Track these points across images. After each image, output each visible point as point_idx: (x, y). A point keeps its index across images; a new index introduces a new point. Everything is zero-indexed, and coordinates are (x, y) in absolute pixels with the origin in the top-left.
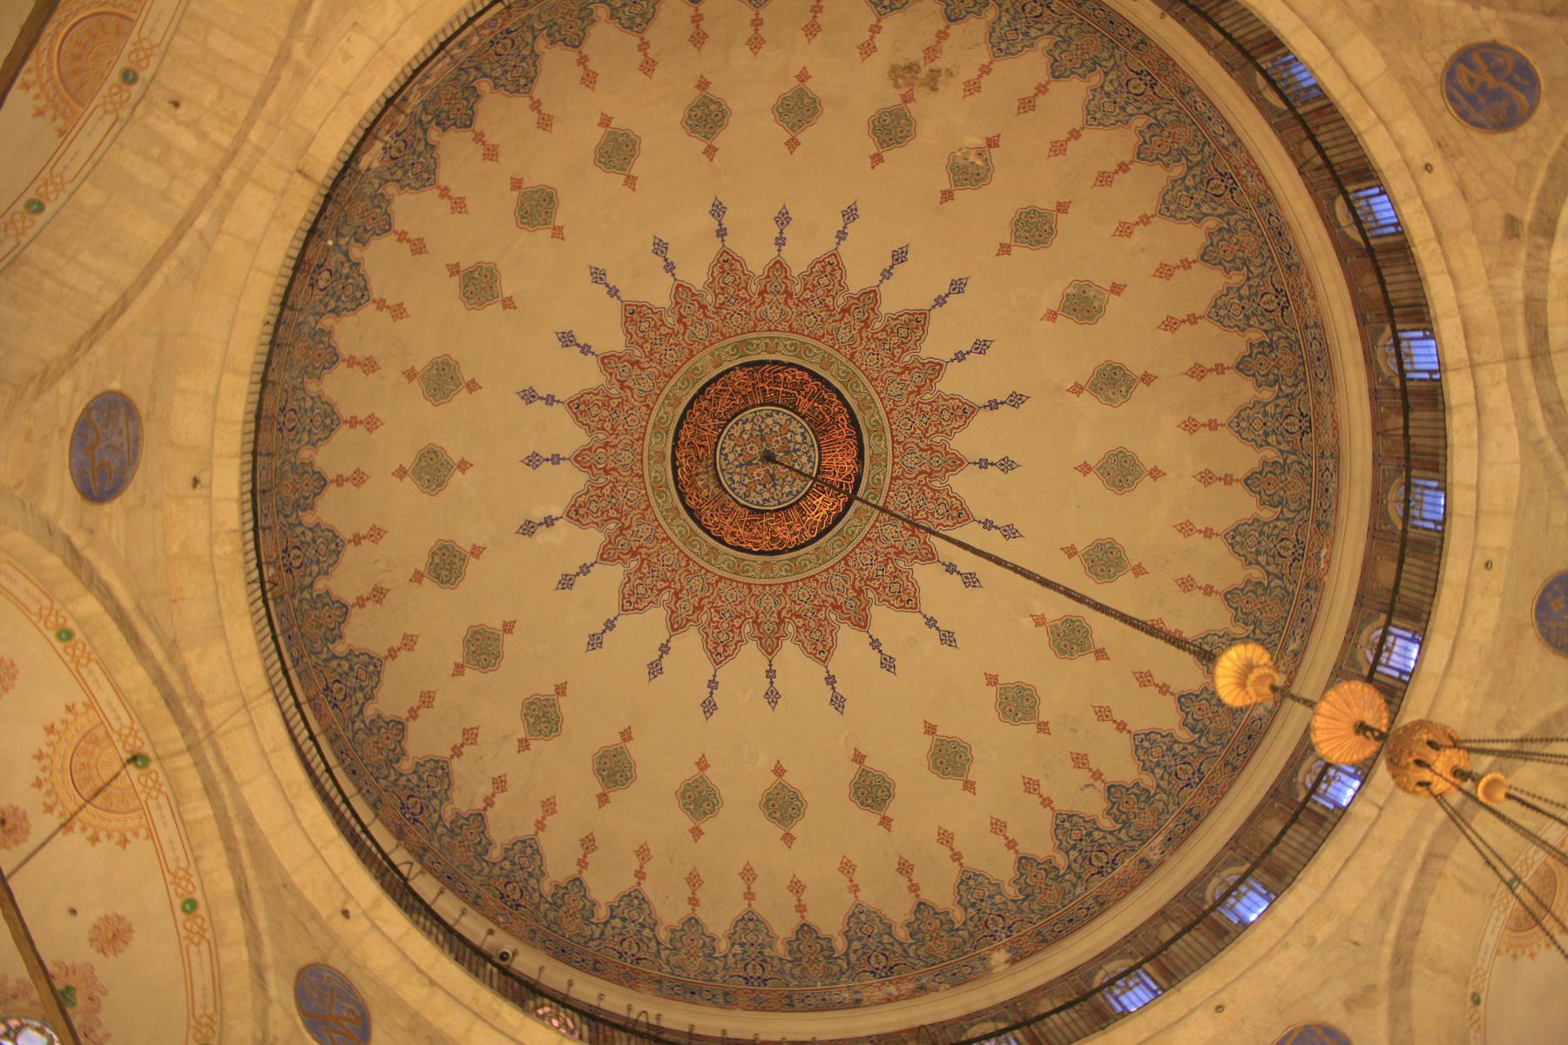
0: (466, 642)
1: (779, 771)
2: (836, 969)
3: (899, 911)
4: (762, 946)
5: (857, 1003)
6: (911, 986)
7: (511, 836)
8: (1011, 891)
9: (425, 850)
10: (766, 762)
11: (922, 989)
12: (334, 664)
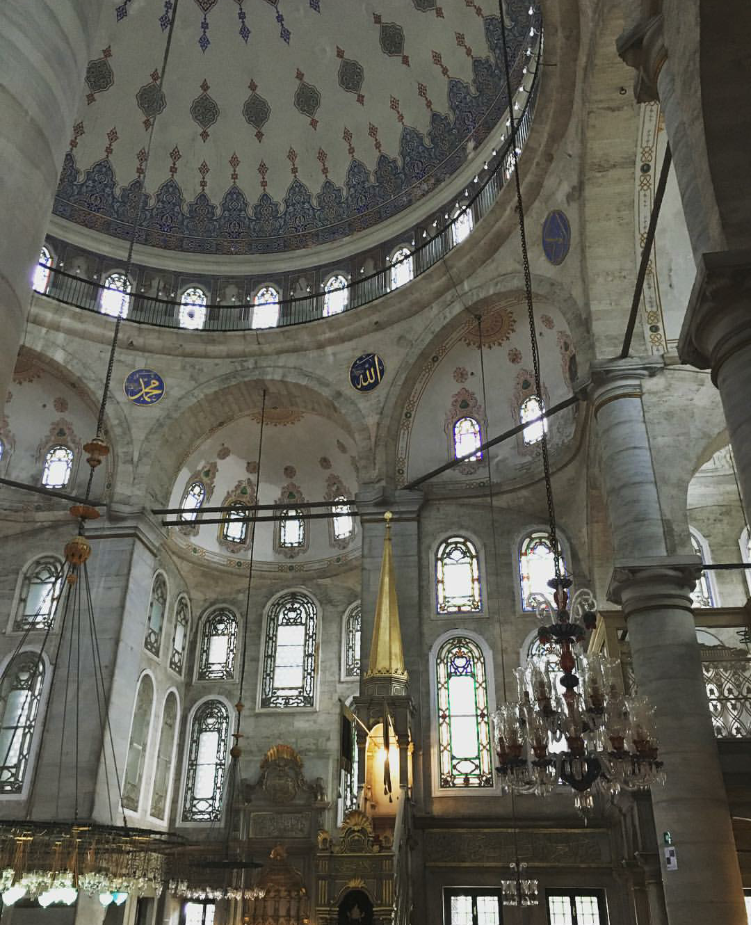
0: (141, 105)
1: (340, 54)
2: (399, 181)
3: (423, 125)
4: (364, 182)
5: (410, 203)
6: (433, 181)
7: (222, 195)
8: (473, 89)
9: (182, 241)
10: (331, 53)
11: (438, 181)
12: (84, 189)
